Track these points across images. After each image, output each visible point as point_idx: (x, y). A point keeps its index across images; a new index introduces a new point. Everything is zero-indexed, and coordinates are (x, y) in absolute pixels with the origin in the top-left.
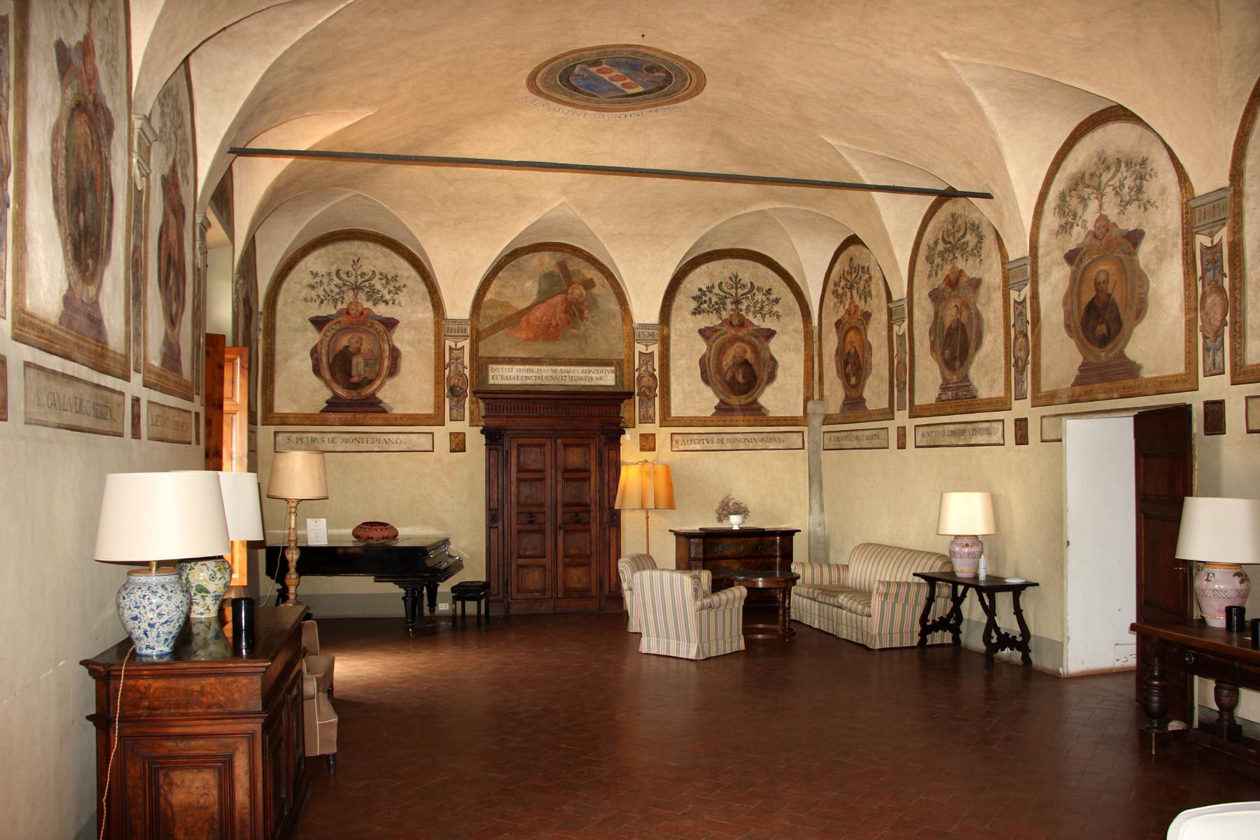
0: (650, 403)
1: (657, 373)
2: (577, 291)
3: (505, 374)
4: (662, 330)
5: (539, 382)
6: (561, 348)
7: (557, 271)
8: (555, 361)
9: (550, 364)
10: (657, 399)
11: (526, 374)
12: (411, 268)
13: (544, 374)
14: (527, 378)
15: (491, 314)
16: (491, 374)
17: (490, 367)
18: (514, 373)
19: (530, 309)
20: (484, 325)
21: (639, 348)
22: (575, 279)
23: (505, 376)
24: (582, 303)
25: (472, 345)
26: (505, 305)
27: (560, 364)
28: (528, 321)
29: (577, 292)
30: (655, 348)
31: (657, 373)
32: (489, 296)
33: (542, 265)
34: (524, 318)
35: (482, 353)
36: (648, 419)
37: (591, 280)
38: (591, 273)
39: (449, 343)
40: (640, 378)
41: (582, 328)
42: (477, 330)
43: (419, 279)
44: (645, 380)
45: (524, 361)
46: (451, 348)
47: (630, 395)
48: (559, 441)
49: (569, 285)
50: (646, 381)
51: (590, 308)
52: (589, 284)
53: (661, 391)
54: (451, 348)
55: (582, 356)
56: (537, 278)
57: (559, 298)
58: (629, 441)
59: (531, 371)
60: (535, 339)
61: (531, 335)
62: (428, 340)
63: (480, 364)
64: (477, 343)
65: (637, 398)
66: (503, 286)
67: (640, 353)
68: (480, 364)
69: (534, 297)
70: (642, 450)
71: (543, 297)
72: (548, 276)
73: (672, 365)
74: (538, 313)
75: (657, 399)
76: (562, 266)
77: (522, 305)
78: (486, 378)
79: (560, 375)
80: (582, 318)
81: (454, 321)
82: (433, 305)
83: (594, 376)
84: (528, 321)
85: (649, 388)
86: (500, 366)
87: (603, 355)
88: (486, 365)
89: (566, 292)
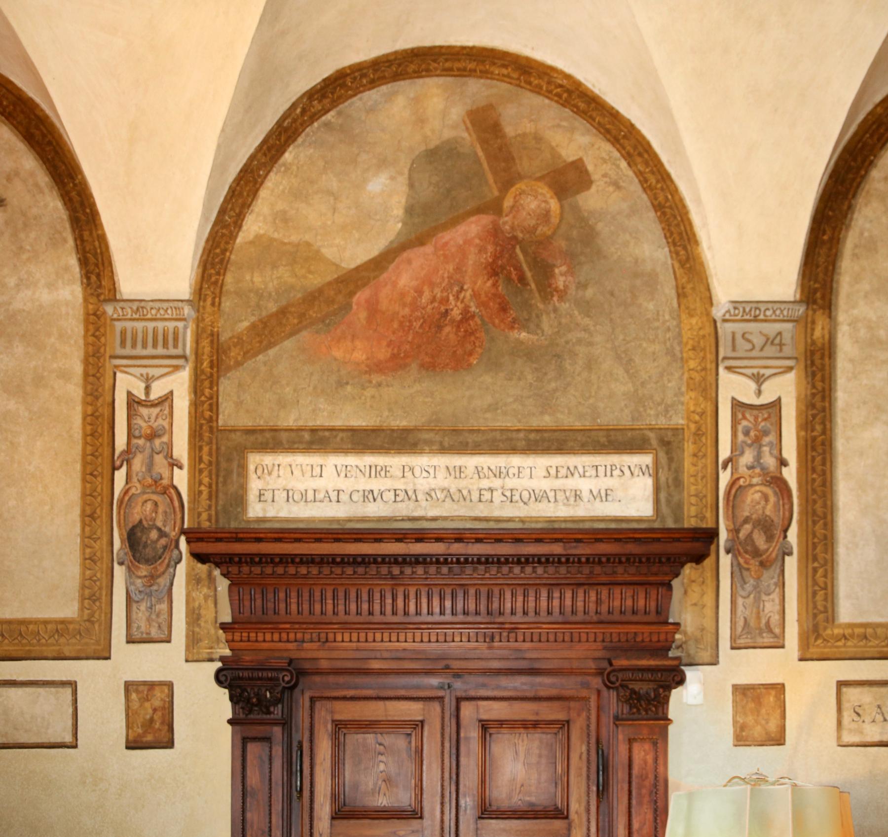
0: (769, 577)
1: (790, 474)
2: (533, 202)
3: (300, 484)
4: (806, 324)
5: (405, 509)
6: (476, 395)
7: (467, 137)
8: (458, 440)
9: (444, 450)
10: (792, 564)
11: (365, 484)
12: (20, 146)
13: (423, 484)
14: (369, 496)
15: (257, 283)
16: (254, 485)
17: (254, 460)
18: (329, 481)
19: (380, 263)
20: (236, 321)
21: (734, 387)
22: (524, 165)
23: (297, 490)
24: (545, 242)
25: (196, 389)
26: (303, 255)
27: (477, 449)
28: (373, 309)
29: (531, 204)
30: (786, 388)
31: (790, 474)
32: (254, 225)
33: (421, 121)
34: (361, 296)
35: (230, 415)
36: (759, 635)
37: (578, 166)
38: (577, 143)
39: (127, 383)
40: (736, 490)
41: (547, 324)
42: (214, 337)
43: (43, 178)
44: (753, 496)
45: (361, 440)
46: (133, 402)
47: (698, 544)
48: (468, 711)
49: (506, 185)
50: (757, 500)
51: (571, 258)
52: (569, 179)
53: (806, 533)
54: (133, 402)
55: (547, 421)
56: (405, 164)
57: (473, 228)
58: (698, 703)
59: (376, 472)
60: (396, 363)
61: (383, 353)
62: (64, 375)
63: (222, 451)
64: (214, 382)
65: (725, 561)
66: (298, 195)
67: (737, 405)
68: (222, 451)
69: (393, 228)
70: (741, 739)
71: (424, 225)
72: (438, 156)
73: (840, 445)
74: (405, 277)
75: (792, 564)
76: (485, 123)
77: (355, 253)
78: (240, 500)
79: (474, 484)
80: (547, 290)
81: (140, 306)
82: (83, 262)
83: (585, 485)
84: (373, 309)
85: (765, 526)
86: (284, 459)
87: (616, 414)
88: (242, 452)
89: (495, 207)
